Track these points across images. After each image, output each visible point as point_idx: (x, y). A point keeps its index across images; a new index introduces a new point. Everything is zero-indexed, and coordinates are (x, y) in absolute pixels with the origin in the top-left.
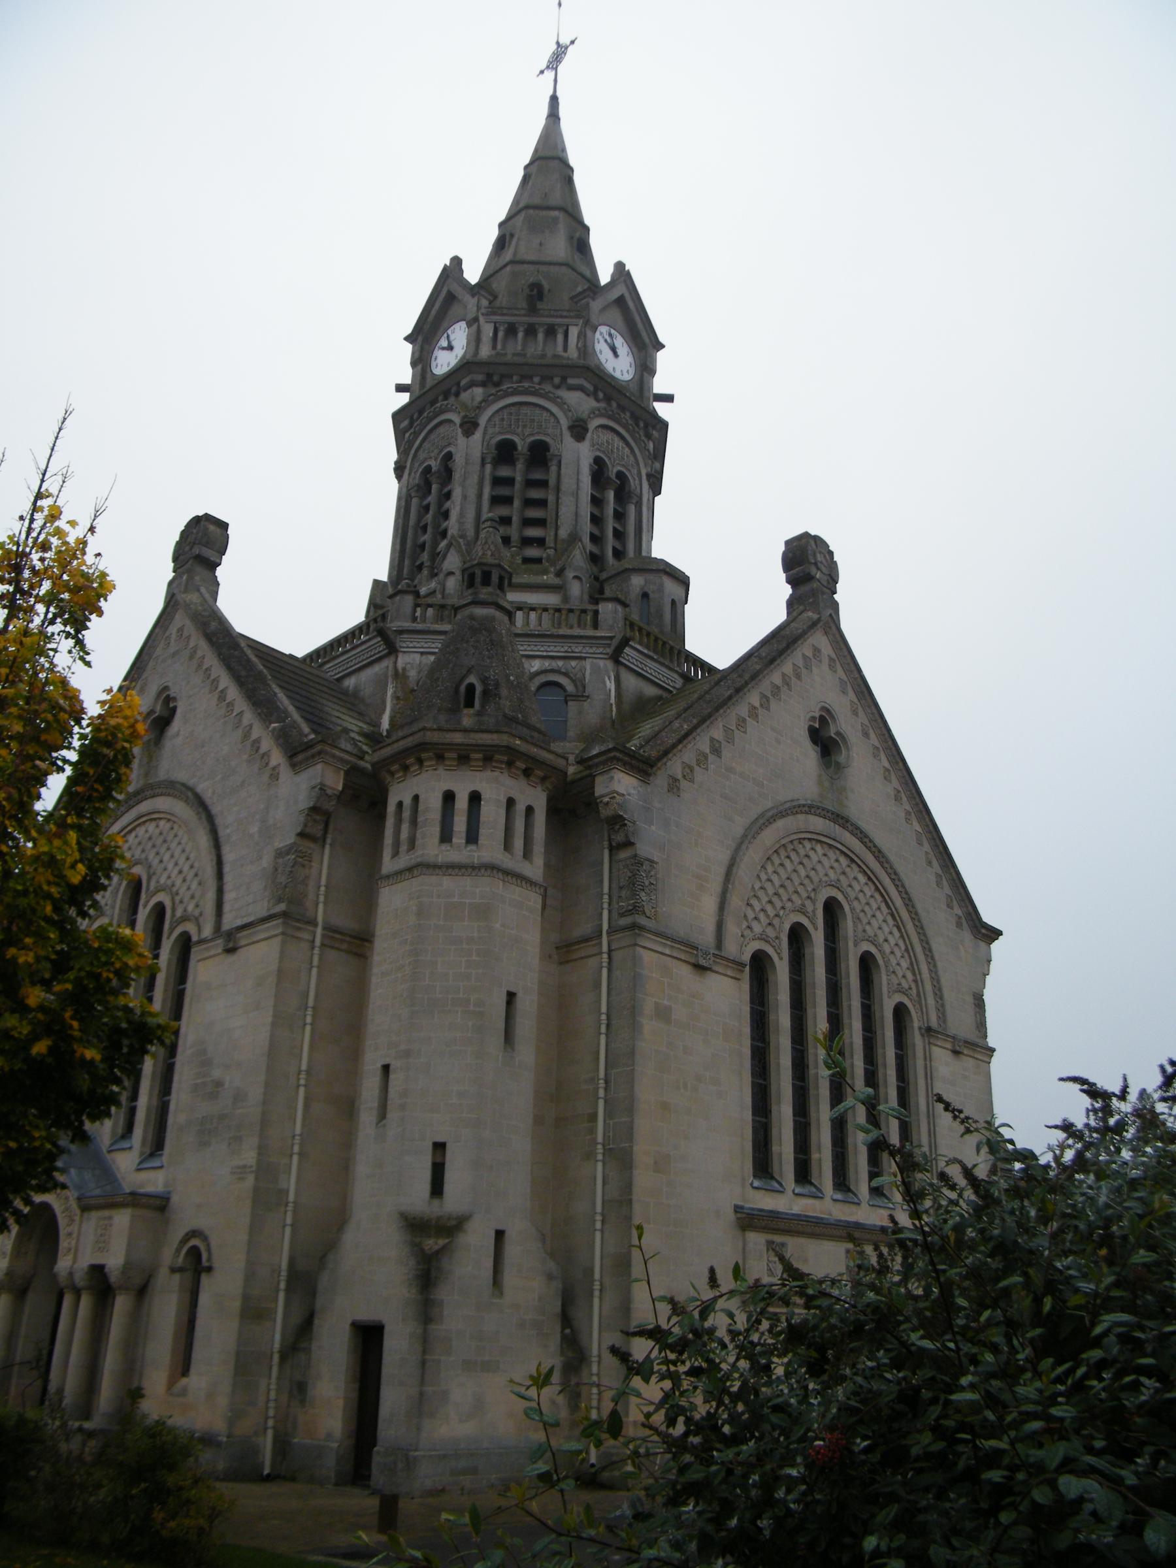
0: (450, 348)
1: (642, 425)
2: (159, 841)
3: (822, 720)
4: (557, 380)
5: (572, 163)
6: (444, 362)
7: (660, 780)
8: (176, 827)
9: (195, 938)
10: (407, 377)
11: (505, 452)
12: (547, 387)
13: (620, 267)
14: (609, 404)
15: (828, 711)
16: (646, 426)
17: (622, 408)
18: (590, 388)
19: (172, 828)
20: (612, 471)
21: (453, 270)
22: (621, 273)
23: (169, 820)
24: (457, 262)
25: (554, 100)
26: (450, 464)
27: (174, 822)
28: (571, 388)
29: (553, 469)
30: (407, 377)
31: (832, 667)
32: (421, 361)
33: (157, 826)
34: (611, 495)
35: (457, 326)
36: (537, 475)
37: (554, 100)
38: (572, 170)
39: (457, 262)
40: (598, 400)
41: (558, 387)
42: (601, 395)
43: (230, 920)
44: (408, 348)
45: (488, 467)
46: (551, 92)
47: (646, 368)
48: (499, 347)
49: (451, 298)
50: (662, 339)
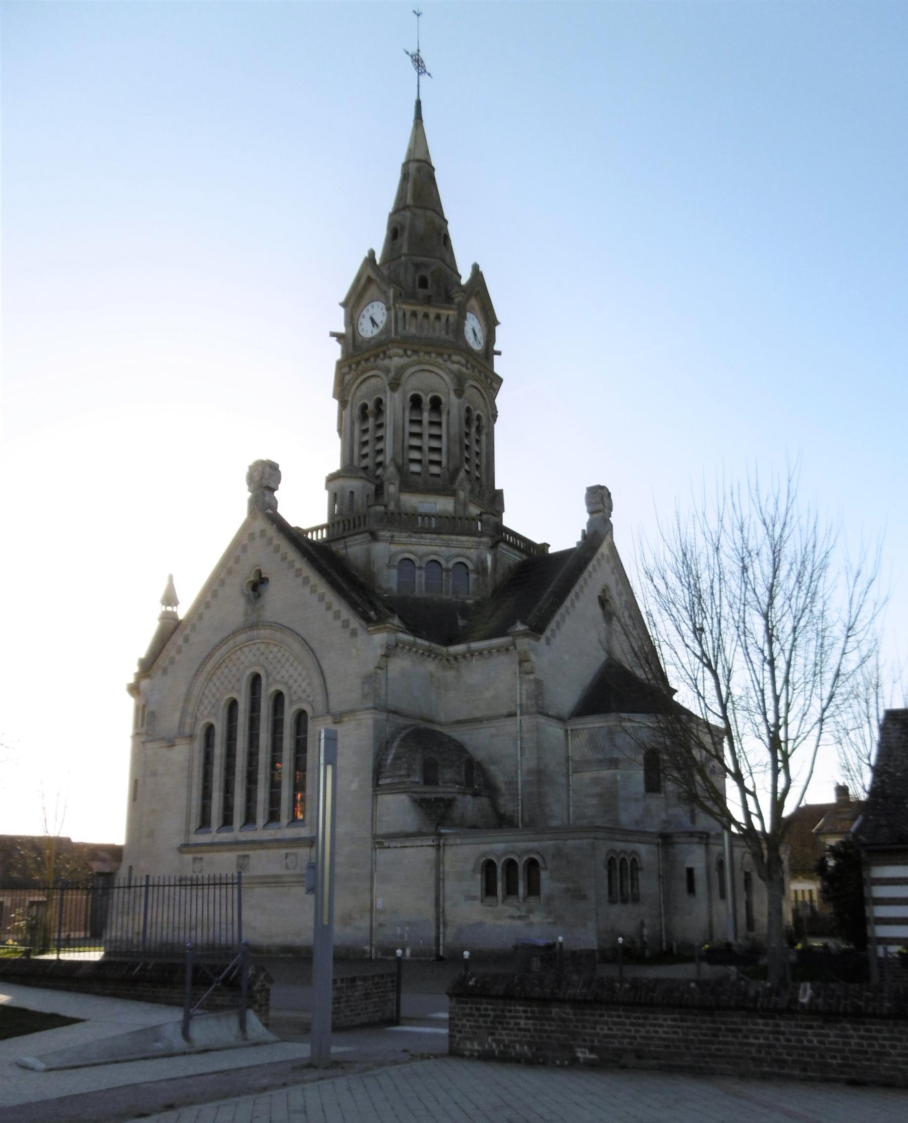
0: (373, 322)
1: (489, 381)
2: (283, 660)
3: (604, 591)
4: (446, 357)
5: (434, 164)
6: (367, 331)
7: (543, 640)
8: (282, 650)
9: (310, 713)
10: (342, 329)
11: (416, 402)
12: (440, 360)
13: (476, 268)
14: (473, 371)
15: (607, 587)
16: (492, 381)
17: (480, 372)
18: (463, 361)
19: (279, 651)
20: (475, 413)
21: (370, 259)
22: (477, 273)
23: (276, 645)
24: (372, 253)
25: (418, 104)
26: (382, 408)
27: (281, 647)
28: (453, 362)
29: (444, 417)
30: (342, 329)
31: (608, 562)
32: (352, 320)
33: (267, 647)
34: (473, 430)
35: (376, 304)
36: (435, 419)
37: (418, 104)
38: (434, 169)
39: (372, 253)
40: (467, 369)
41: (445, 361)
42: (469, 366)
43: (336, 705)
44: (341, 312)
45: (407, 413)
46: (415, 98)
47: (490, 338)
48: (407, 327)
49: (369, 280)
50: (499, 318)
